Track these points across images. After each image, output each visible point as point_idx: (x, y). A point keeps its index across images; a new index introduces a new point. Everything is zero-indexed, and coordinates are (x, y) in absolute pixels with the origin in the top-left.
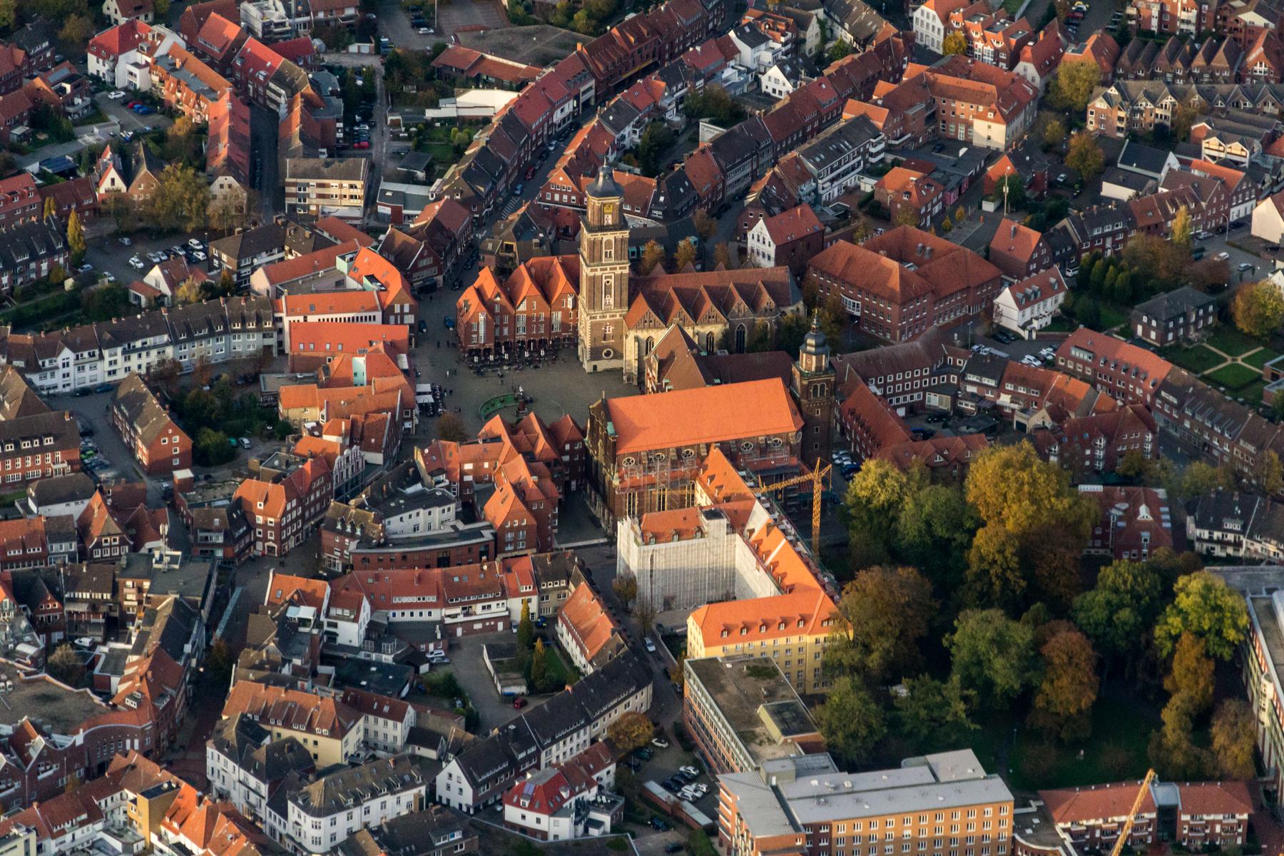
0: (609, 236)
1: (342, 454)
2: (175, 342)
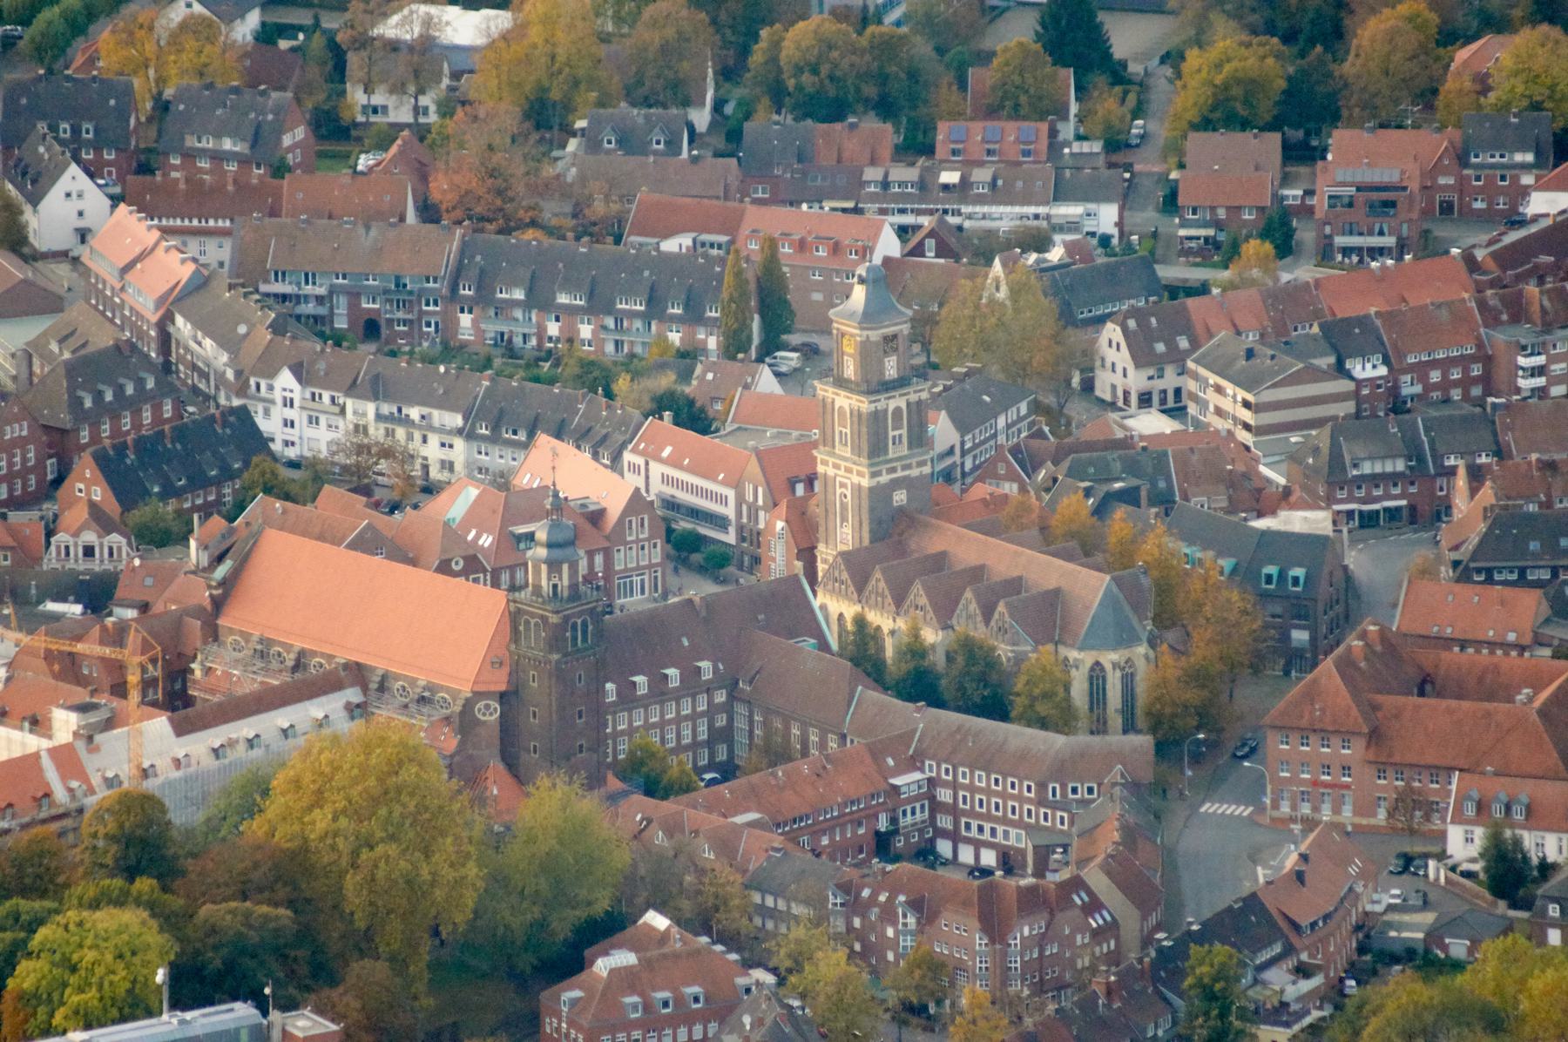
0: (845, 401)
1: (76, 534)
2: (468, 434)
